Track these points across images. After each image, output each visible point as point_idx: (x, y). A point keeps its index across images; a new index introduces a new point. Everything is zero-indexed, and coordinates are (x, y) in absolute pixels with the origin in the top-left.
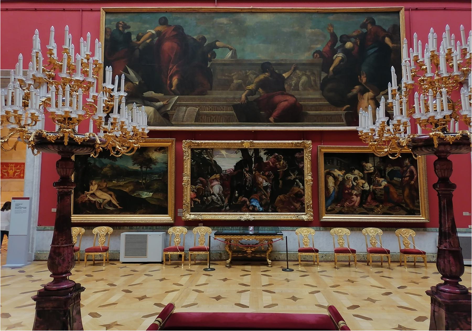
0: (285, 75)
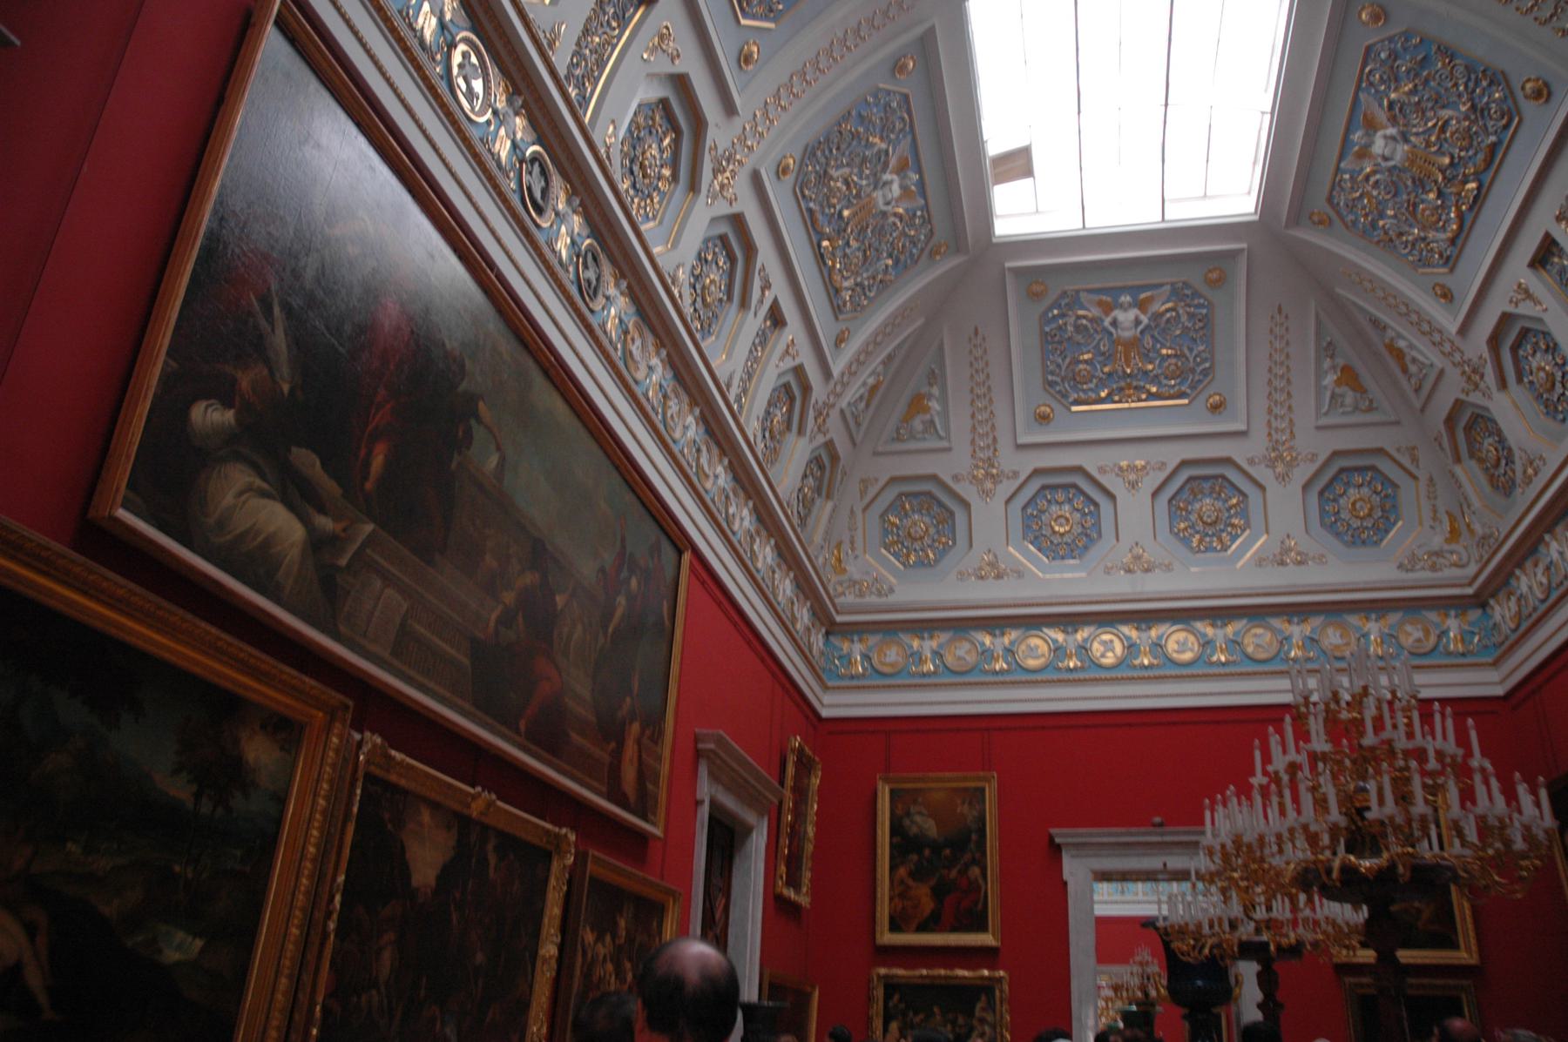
0: (560, 600)
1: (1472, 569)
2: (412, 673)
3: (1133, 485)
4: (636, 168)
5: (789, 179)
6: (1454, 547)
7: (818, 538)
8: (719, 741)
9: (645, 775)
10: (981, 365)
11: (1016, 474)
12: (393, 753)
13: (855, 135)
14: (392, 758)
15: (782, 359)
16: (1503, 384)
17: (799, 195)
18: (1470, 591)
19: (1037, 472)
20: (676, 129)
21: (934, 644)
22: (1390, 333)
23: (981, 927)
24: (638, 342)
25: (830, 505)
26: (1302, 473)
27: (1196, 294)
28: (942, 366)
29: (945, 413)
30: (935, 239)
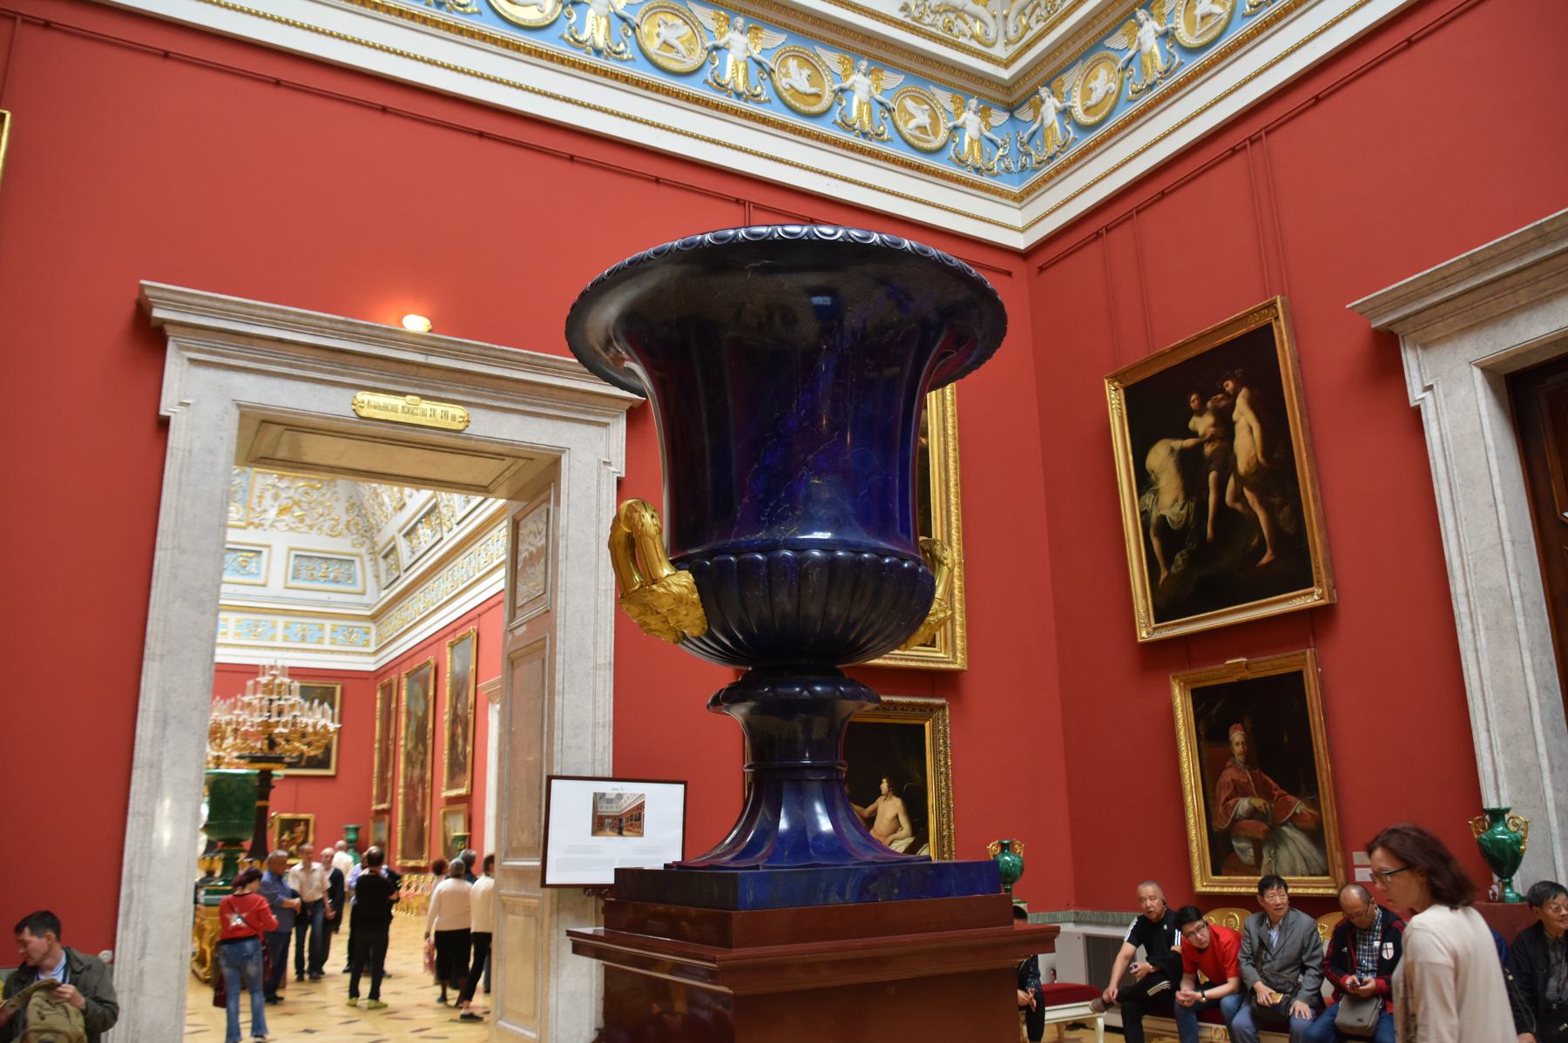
18: (1005, 74)
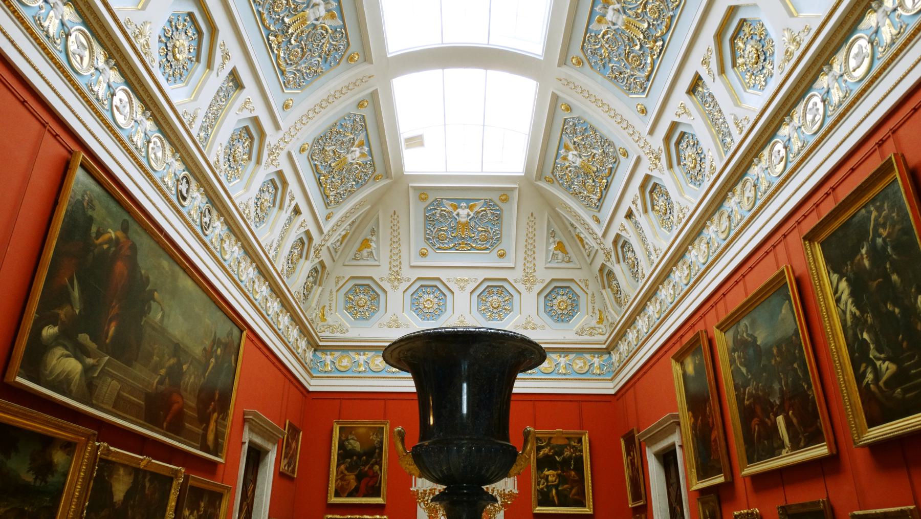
0: (185, 367)
1: (605, 337)
2: (121, 413)
3: (462, 288)
4: (231, 158)
5: (306, 153)
6: (600, 326)
7: (314, 305)
8: (255, 415)
9: (218, 435)
10: (396, 228)
11: (409, 279)
12: (111, 448)
13: (338, 133)
14: (110, 450)
15: (298, 229)
16: (618, 262)
17: (311, 158)
18: (604, 346)
19: (419, 279)
20: (251, 138)
21: (365, 358)
22: (578, 231)
23: (378, 495)
24: (228, 242)
25: (320, 288)
26: (538, 287)
27: (495, 205)
28: (378, 227)
29: (378, 249)
30: (376, 174)
